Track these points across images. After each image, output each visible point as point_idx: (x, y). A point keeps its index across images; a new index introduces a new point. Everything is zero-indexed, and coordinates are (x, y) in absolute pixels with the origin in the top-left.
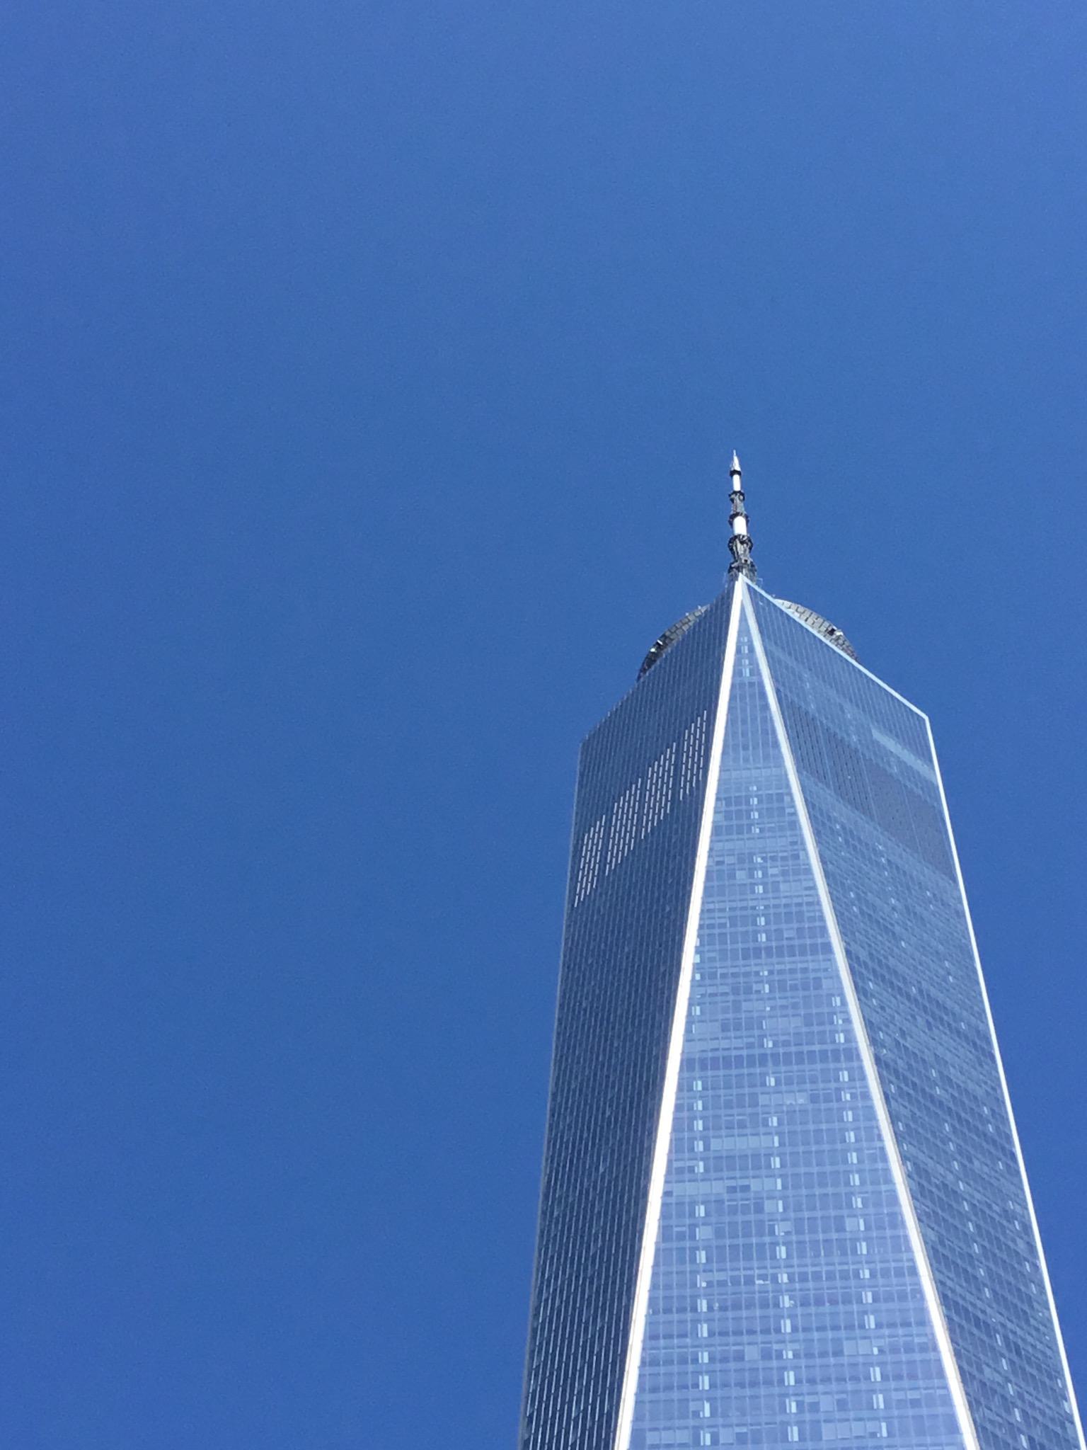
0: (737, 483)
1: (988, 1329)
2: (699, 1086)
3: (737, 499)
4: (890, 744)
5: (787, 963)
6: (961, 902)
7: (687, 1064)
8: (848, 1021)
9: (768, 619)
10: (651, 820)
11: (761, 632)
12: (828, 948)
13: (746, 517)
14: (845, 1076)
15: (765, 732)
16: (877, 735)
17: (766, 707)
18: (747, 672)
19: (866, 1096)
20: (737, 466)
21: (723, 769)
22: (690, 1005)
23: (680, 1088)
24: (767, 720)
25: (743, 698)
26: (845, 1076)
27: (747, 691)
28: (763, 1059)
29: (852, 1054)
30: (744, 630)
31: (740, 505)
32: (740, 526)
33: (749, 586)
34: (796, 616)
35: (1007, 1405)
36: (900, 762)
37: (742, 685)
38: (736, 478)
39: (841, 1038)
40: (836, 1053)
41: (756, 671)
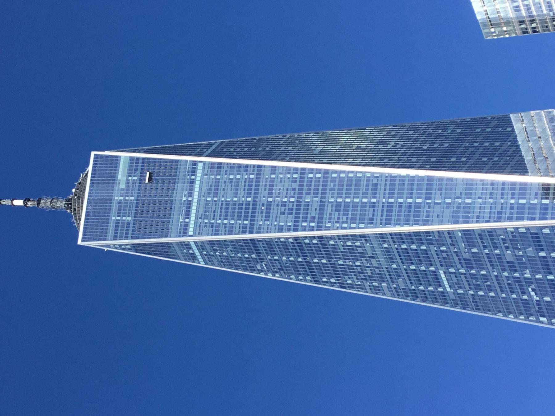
6: (186, 161)
7: (316, 282)
11: (105, 240)
13: (13, 200)
15: (156, 246)
16: (123, 186)
18: (130, 247)
21: (180, 259)
22: (291, 279)
25: (142, 250)
26: (307, 241)
29: (296, 239)
32: (19, 203)
33: (82, 241)
35: (418, 205)
36: (129, 174)
37: (136, 250)
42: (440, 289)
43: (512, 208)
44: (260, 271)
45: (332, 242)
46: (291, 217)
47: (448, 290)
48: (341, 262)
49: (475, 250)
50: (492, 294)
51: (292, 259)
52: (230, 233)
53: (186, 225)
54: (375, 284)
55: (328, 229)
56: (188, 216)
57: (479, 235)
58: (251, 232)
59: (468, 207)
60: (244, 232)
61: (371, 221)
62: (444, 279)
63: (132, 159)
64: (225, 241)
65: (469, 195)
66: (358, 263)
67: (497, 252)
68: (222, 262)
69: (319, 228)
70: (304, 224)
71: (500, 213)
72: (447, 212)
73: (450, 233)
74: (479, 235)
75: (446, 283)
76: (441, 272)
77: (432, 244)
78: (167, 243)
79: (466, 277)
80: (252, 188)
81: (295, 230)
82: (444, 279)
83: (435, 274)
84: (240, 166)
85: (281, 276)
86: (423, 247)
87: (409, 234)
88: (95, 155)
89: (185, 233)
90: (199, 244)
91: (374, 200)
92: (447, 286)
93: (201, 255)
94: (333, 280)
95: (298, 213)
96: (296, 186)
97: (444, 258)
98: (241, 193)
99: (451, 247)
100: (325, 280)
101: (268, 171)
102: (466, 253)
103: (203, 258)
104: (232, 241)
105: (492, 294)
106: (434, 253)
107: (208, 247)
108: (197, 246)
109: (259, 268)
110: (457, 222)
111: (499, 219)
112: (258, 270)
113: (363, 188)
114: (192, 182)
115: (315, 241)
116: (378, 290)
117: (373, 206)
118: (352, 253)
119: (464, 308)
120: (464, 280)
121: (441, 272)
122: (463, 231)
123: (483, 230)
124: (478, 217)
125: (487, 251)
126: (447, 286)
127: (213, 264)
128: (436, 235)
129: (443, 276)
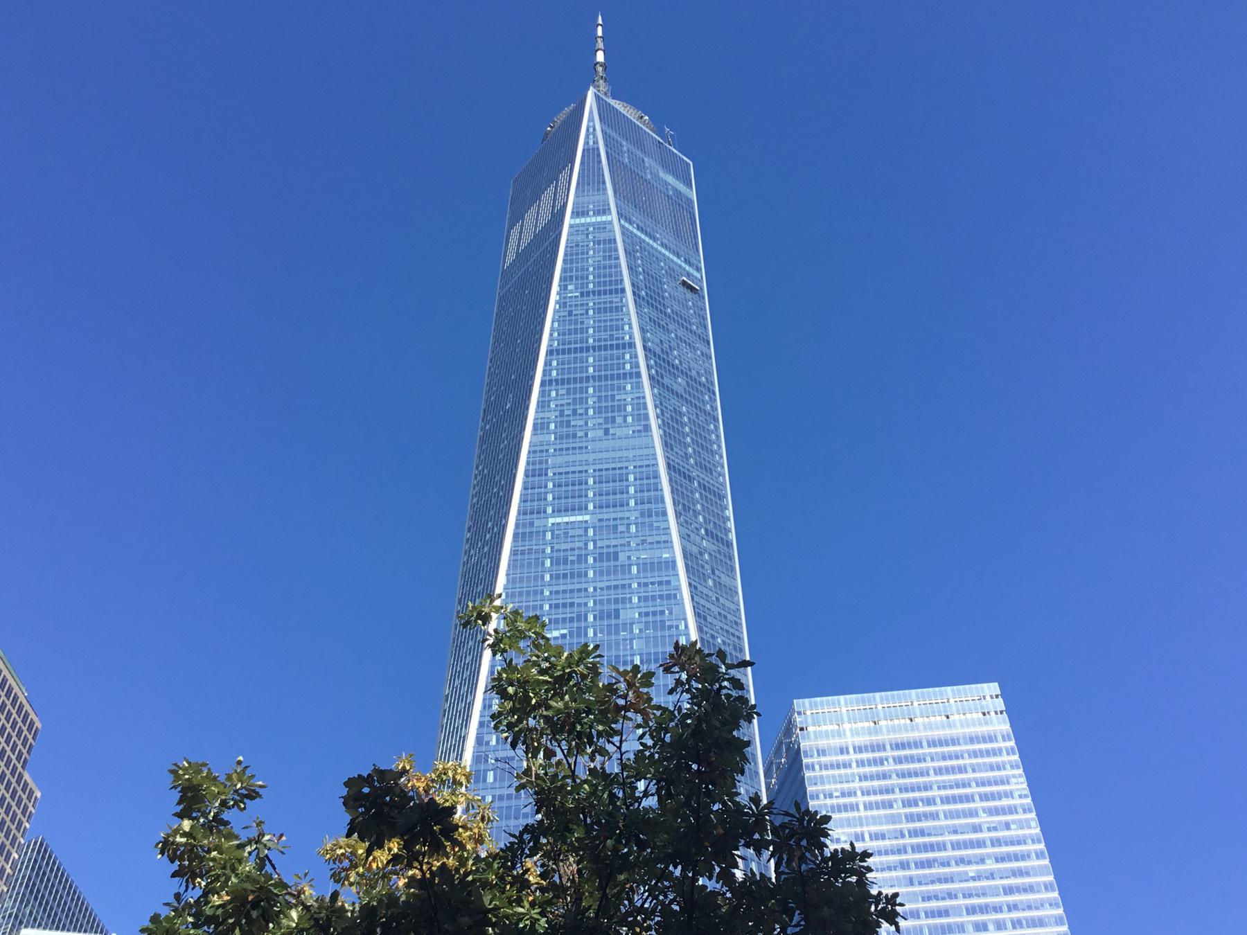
0: (600, 31)
1: (691, 479)
2: (554, 363)
3: (599, 40)
4: (670, 179)
5: (603, 298)
7: (550, 352)
8: (631, 328)
9: (605, 112)
10: (542, 222)
12: (623, 290)
14: (627, 357)
16: (662, 174)
17: (600, 162)
19: (637, 366)
20: (600, 22)
21: (577, 196)
23: (546, 364)
24: (600, 169)
26: (627, 357)
27: (591, 152)
28: (588, 349)
29: (632, 345)
30: (591, 119)
31: (600, 44)
32: (600, 57)
34: (621, 110)
35: (696, 514)
38: (600, 28)
39: (627, 337)
40: (624, 345)
41: (596, 142)
42: (549, 510)
43: (713, 637)
44: (563, 287)
45: (629, 387)
46: (658, 350)
47: (551, 521)
48: (591, 390)
49: (634, 569)
50: (547, 578)
51: (591, 331)
52: (630, 268)
53: (630, 222)
54: (552, 426)
55: (652, 387)
56: (638, 228)
57: (668, 582)
58: (634, 293)
59: (705, 578)
60: (633, 285)
61: (667, 445)
62: (573, 519)
63: (692, 202)
64: (617, 258)
65: (718, 584)
66: (591, 412)
67: (635, 600)
68: (577, 246)
69: (651, 377)
70: (652, 362)
71: (705, 619)
72: (695, 550)
73: (668, 543)
74: (668, 582)
75: (566, 519)
76: (587, 518)
77: (642, 515)
78: (605, 189)
79: (579, 548)
80: (682, 321)
81: (645, 348)
82: (573, 519)
83: (582, 509)
84: (705, 319)
85: (555, 311)
86: (632, 503)
87: (657, 488)
88: (688, 165)
89: (620, 215)
90: (608, 227)
91: (692, 461)
92: (559, 520)
93: (589, 224)
94: (554, 373)
95: (661, 361)
96: (694, 373)
97: (615, 527)
98: (676, 307)
99: (638, 540)
100: (554, 363)
101: (705, 350)
102: (629, 558)
103: (583, 225)
104: (618, 266)
105: (547, 578)
106: (626, 515)
107: (602, 236)
108: (604, 223)
109: (570, 287)
110: (685, 557)
111: (697, 615)
112: (566, 286)
113: (704, 455)
114: (678, 256)
115: (628, 366)
116: (539, 427)
117: (687, 456)
118: (610, 412)
119: (516, 535)
120: (577, 545)
121: (587, 518)
122: (674, 562)
123: (678, 588)
124: (696, 588)
125: (635, 585)
126: (559, 520)
127: (570, 234)
128: (663, 525)
129: (580, 518)
